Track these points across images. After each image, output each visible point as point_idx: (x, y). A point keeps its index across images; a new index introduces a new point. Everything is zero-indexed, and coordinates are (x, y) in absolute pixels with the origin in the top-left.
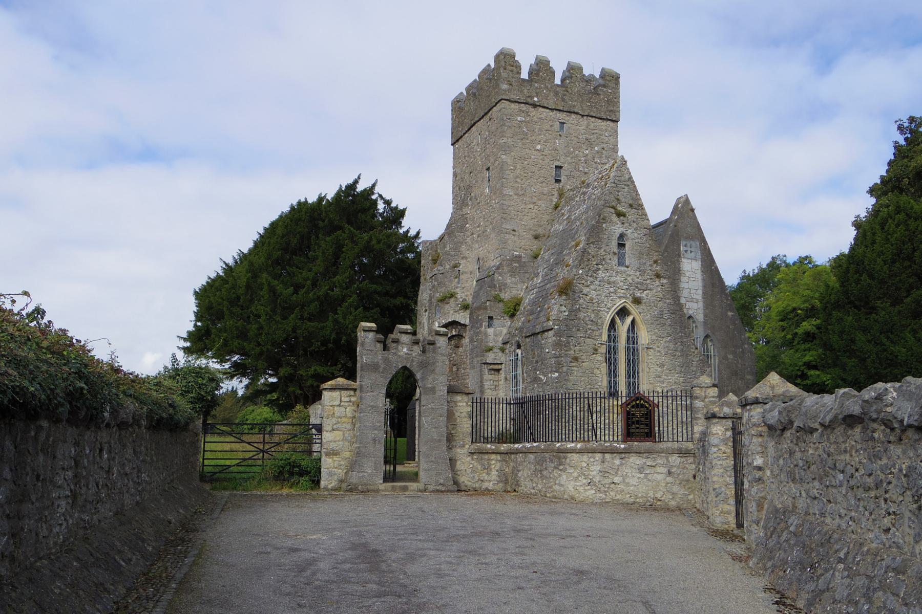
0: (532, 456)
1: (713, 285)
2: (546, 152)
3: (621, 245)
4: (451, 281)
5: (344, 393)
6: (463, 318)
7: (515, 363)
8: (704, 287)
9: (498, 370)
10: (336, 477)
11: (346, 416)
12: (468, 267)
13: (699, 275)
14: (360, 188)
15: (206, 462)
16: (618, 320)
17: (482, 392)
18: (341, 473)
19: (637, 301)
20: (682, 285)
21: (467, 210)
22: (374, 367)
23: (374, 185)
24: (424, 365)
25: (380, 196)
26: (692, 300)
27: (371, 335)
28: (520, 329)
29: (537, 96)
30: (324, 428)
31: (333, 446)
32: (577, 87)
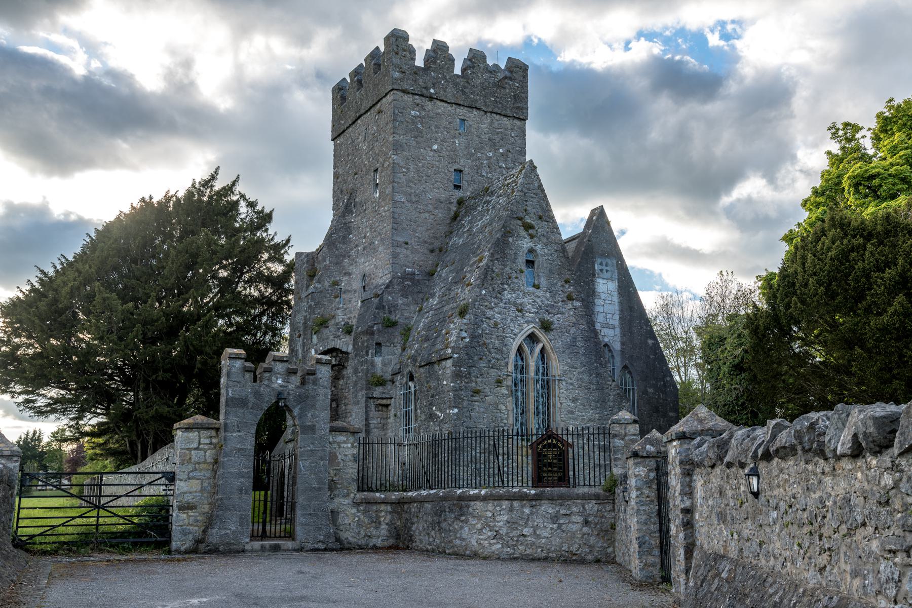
0: (428, 506)
4: (330, 301)
5: (204, 433)
6: (345, 343)
7: (407, 397)
8: (621, 311)
9: (387, 406)
10: (191, 537)
11: (205, 462)
13: (616, 299)
15: (22, 523)
17: (368, 432)
18: (196, 530)
20: (598, 309)
23: (234, 184)
24: (302, 399)
25: (243, 196)
26: (608, 326)
27: (238, 364)
28: (414, 359)
29: (434, 87)
30: (177, 477)
31: (188, 498)
32: (480, 79)
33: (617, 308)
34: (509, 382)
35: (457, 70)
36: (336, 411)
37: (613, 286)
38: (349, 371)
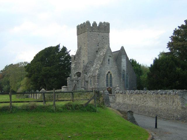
3: (109, 61)
13: (125, 62)
26: (124, 67)
35: (98, 26)
37: (125, 60)
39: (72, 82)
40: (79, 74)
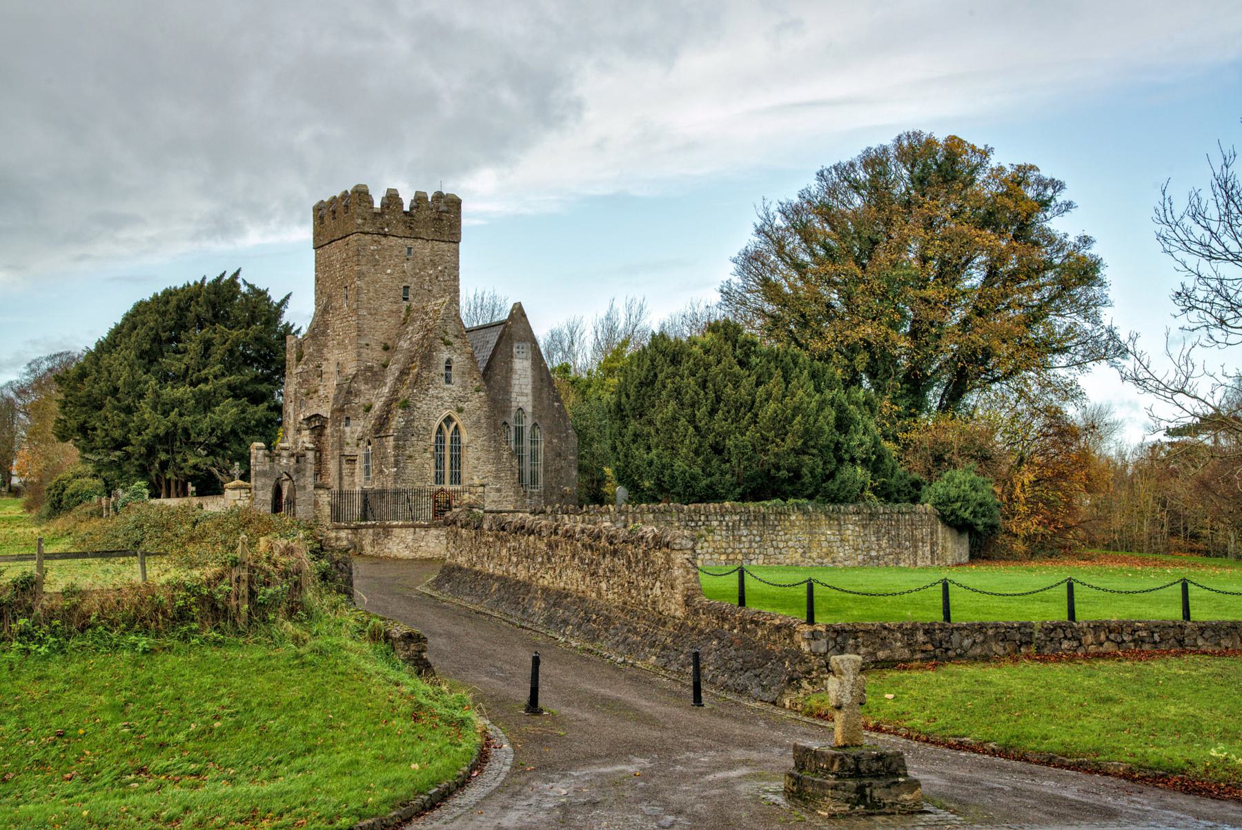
0: (371, 531)
1: (542, 380)
2: (396, 275)
3: (448, 368)
7: (367, 457)
12: (329, 367)
13: (529, 373)
14: (227, 277)
16: (445, 426)
19: (460, 410)
20: (514, 382)
21: (329, 317)
22: (264, 474)
26: (522, 394)
27: (261, 452)
32: (425, 214)
33: (530, 380)
34: (432, 449)
35: (406, 208)
36: (319, 472)
37: (527, 364)
38: (328, 431)
39: (273, 461)
40: (317, 425)
